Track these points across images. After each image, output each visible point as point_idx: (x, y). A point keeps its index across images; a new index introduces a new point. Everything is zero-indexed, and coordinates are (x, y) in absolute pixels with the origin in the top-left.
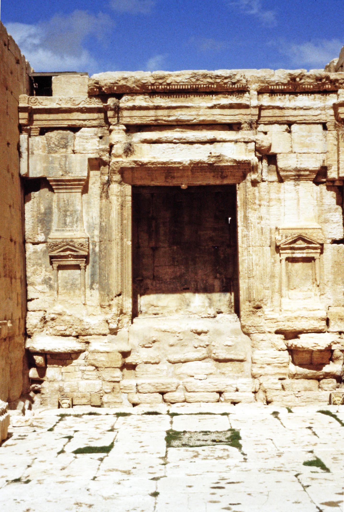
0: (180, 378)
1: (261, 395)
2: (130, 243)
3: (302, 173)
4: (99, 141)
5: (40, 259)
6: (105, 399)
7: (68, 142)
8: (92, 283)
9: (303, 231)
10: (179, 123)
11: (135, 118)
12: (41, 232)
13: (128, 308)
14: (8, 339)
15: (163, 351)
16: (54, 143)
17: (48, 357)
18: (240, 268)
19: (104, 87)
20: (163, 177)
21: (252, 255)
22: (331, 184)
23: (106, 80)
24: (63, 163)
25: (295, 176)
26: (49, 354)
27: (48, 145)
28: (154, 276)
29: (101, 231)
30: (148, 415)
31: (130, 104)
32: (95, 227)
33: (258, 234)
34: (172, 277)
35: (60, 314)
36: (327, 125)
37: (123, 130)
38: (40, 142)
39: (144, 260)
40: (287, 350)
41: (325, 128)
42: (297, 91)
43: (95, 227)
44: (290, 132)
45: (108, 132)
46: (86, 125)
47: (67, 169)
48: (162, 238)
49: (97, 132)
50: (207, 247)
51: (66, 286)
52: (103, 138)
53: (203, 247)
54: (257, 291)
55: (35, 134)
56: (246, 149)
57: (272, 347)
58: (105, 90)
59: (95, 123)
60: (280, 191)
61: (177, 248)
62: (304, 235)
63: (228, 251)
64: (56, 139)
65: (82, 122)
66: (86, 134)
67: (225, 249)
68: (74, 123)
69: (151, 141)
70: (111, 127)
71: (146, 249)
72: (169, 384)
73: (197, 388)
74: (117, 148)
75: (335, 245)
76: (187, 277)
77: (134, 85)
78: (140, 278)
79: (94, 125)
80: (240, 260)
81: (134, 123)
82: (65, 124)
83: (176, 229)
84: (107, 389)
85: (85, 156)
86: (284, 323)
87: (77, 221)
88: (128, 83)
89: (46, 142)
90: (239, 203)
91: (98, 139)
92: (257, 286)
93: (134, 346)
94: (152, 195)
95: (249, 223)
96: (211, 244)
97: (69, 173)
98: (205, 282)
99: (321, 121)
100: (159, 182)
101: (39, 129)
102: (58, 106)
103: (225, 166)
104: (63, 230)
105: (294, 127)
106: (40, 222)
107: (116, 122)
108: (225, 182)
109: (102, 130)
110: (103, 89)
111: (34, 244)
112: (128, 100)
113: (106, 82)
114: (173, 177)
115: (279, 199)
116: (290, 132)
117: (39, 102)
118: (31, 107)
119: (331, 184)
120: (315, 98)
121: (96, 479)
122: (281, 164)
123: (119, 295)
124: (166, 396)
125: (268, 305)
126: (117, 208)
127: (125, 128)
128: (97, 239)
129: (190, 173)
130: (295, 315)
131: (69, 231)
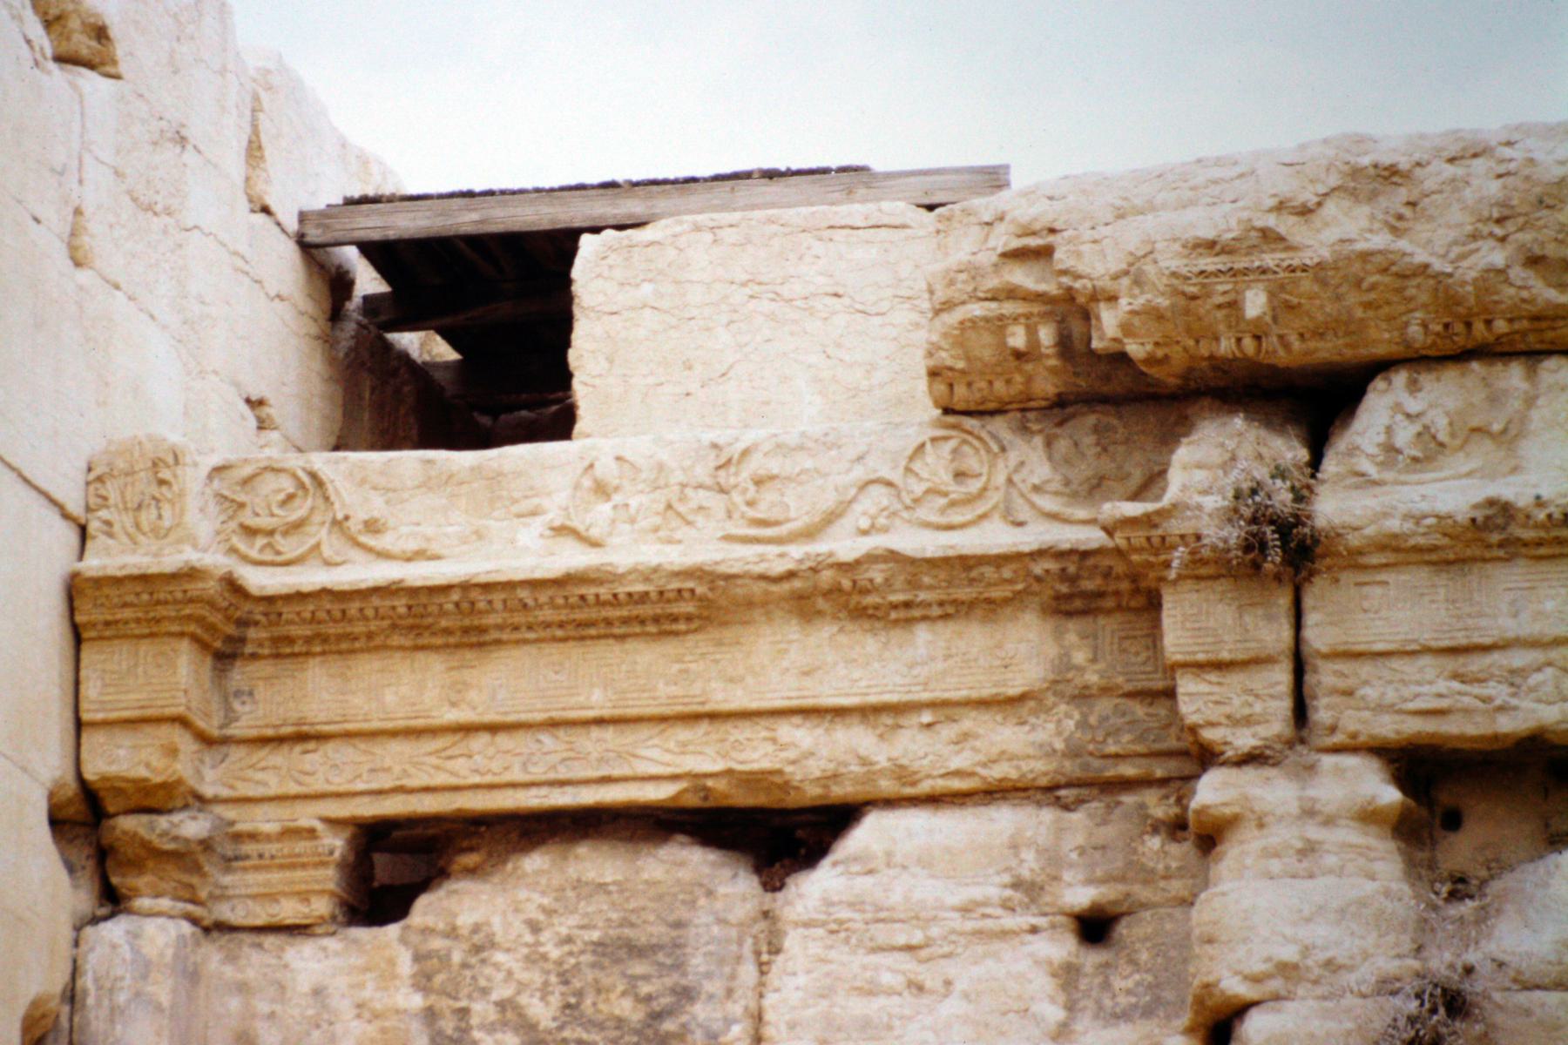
4: (1067, 975)
7: (686, 994)
11: (1519, 659)
19: (1113, 299)
23: (1150, 207)
31: (1452, 493)
37: (1369, 816)
38: (345, 1007)
45: (1181, 851)
46: (902, 773)
49: (1053, 861)
52: (1122, 929)
58: (1127, 329)
59: (1016, 746)
64: (535, 958)
65: (857, 740)
66: (899, 890)
68: (754, 752)
77: (1498, 257)
79: (997, 772)
81: (1507, 725)
82: (656, 768)
88: (1422, 230)
89: (417, 1001)
91: (1063, 947)
101: (336, 844)
102: (570, 558)
109: (1109, 832)
110: (1109, 322)
112: (1431, 450)
113: (1131, 236)
117: (338, 524)
118: (233, 586)
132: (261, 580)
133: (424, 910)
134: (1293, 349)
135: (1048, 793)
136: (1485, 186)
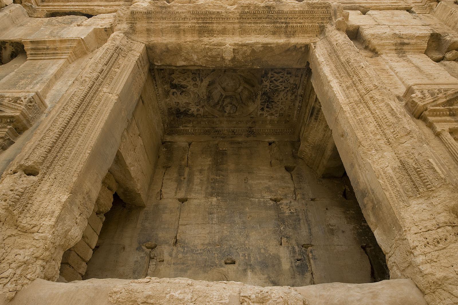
2: (114, 98)
3: (406, 41)
25: (395, 45)
34: (207, 242)
48: (197, 188)
53: (257, 200)
67: (291, 202)
71: (170, 200)
76: (231, 243)
83: (218, 177)
94: (190, 145)
96: (268, 196)
98: (263, 251)
103: (291, 12)
114: (211, 33)
123: (30, 172)
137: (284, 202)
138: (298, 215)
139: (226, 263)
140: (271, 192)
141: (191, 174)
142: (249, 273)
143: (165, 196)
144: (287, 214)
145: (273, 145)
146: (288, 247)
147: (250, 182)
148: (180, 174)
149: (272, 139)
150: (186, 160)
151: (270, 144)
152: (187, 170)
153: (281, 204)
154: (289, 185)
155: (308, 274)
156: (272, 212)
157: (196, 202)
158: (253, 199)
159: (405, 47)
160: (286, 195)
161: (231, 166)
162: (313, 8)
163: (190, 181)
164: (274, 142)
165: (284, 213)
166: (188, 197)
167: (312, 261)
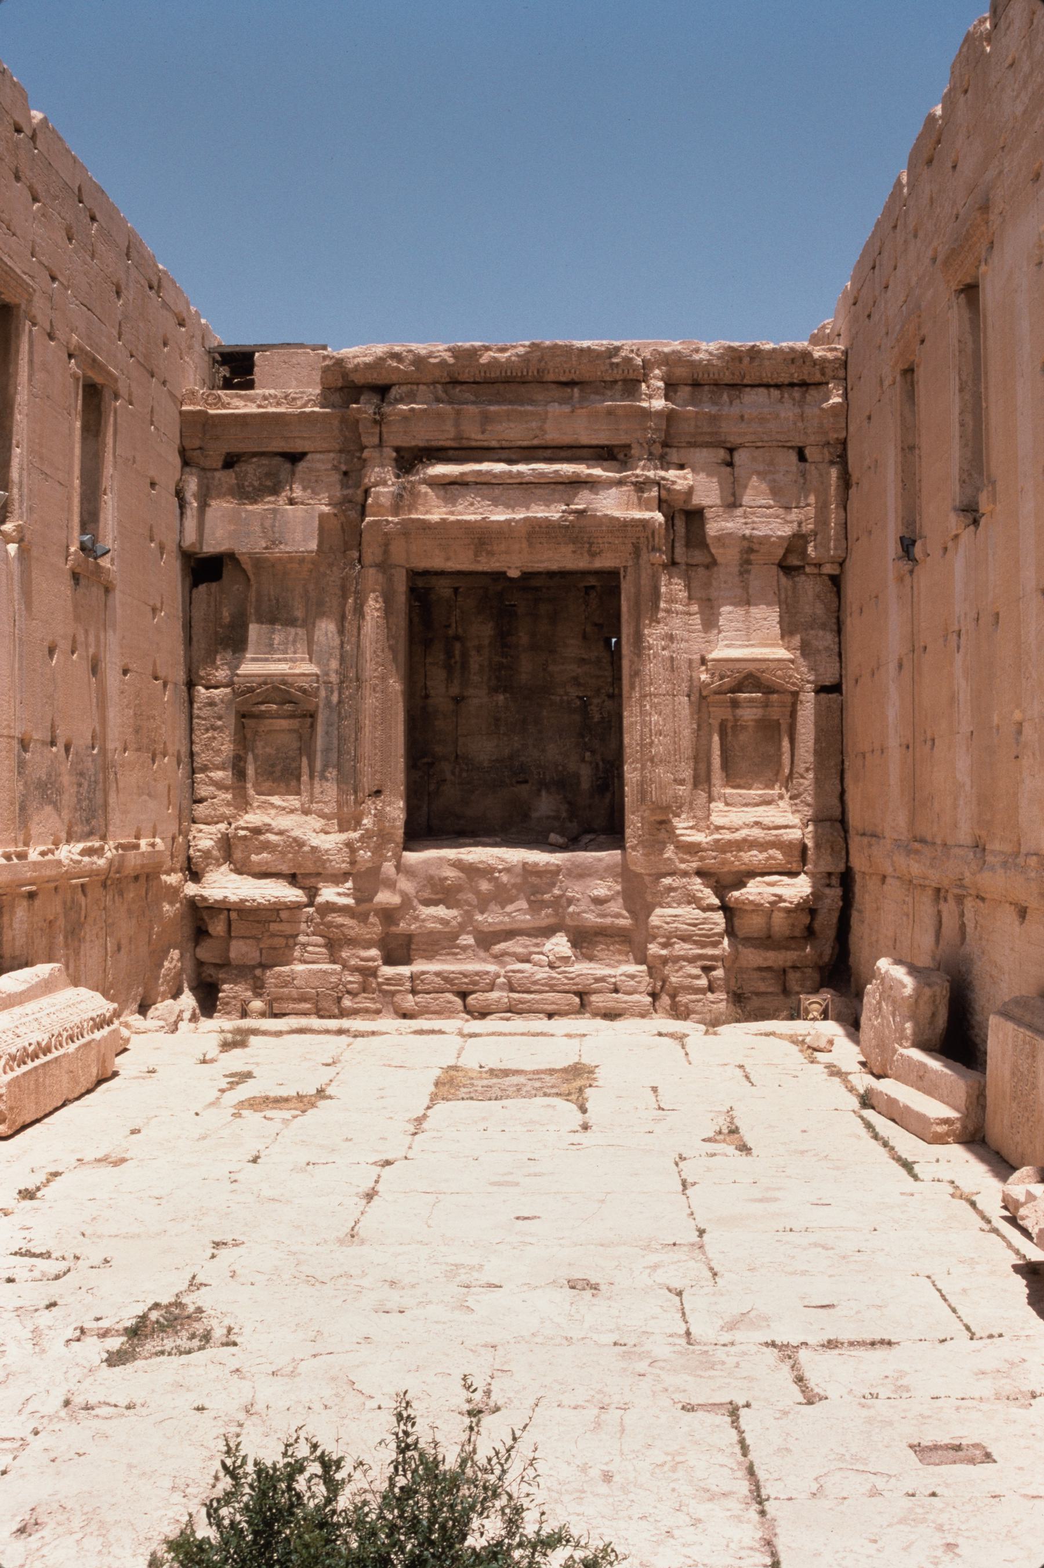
0: (503, 964)
1: (665, 1000)
3: (756, 547)
4: (341, 481)
5: (220, 718)
6: (347, 1002)
8: (326, 766)
9: (757, 665)
10: (505, 444)
12: (222, 664)
13: (394, 820)
14: (143, 880)
15: (466, 908)
16: (253, 486)
17: (234, 915)
18: (626, 740)
20: (471, 553)
21: (650, 714)
22: (816, 571)
24: (268, 523)
26: (235, 910)
27: (239, 487)
28: (457, 756)
29: (342, 660)
30: (418, 1036)
32: (331, 654)
33: (661, 670)
34: (494, 758)
35: (257, 831)
36: (807, 452)
39: (437, 723)
40: (720, 908)
41: (802, 457)
42: (745, 382)
43: (331, 654)
44: (730, 464)
47: (277, 535)
48: (476, 679)
49: (340, 463)
50: (565, 698)
51: (272, 773)
53: (558, 698)
54: (661, 787)
55: (214, 466)
56: (640, 498)
57: (689, 903)
60: (711, 584)
61: (506, 699)
62: (759, 674)
63: (609, 704)
64: (255, 475)
67: (604, 702)
69: (447, 480)
70: (366, 454)
72: (477, 974)
73: (535, 983)
74: (375, 493)
75: (823, 695)
76: (523, 758)
78: (430, 760)
80: (625, 722)
83: (504, 661)
84: (351, 982)
85: (313, 509)
86: (714, 854)
87: (294, 641)
90: (624, 608)
92: (659, 776)
93: (407, 894)
94: (456, 590)
95: (644, 648)
96: (574, 692)
97: (281, 543)
98: (560, 768)
99: (793, 444)
100: (462, 561)
104: (266, 660)
105: (741, 457)
106: (221, 644)
107: (376, 440)
108: (598, 564)
111: (207, 688)
113: (356, 361)
114: (491, 553)
115: (709, 600)
116: (730, 464)
119: (816, 571)
120: (782, 397)
121: (259, 1160)
122: (713, 528)
124: (471, 1000)
125: (683, 816)
126: (376, 614)
127: (394, 454)
128: (334, 678)
129: (525, 545)
130: (738, 836)
131: (279, 660)
132: (211, 412)
133: (237, 469)
134: (381, 381)
135: (341, 451)
136: (410, 357)
137: (595, 701)
138: (610, 721)
139: (518, 782)
140: (579, 685)
141: (465, 655)
142: (544, 793)
143: (432, 692)
144: (596, 720)
145: (593, 594)
146: (591, 763)
147: (551, 668)
148: (449, 654)
149: (592, 581)
150: (454, 625)
151: (586, 587)
152: (458, 646)
153: (590, 704)
154: (606, 673)
155: (608, 795)
156: (577, 717)
157: (476, 701)
158: (553, 697)
159: (752, 557)
160: (599, 690)
161: (524, 639)
162: (626, 526)
163: (465, 666)
164: (593, 587)
165: (593, 718)
166: (465, 694)
167: (616, 780)
